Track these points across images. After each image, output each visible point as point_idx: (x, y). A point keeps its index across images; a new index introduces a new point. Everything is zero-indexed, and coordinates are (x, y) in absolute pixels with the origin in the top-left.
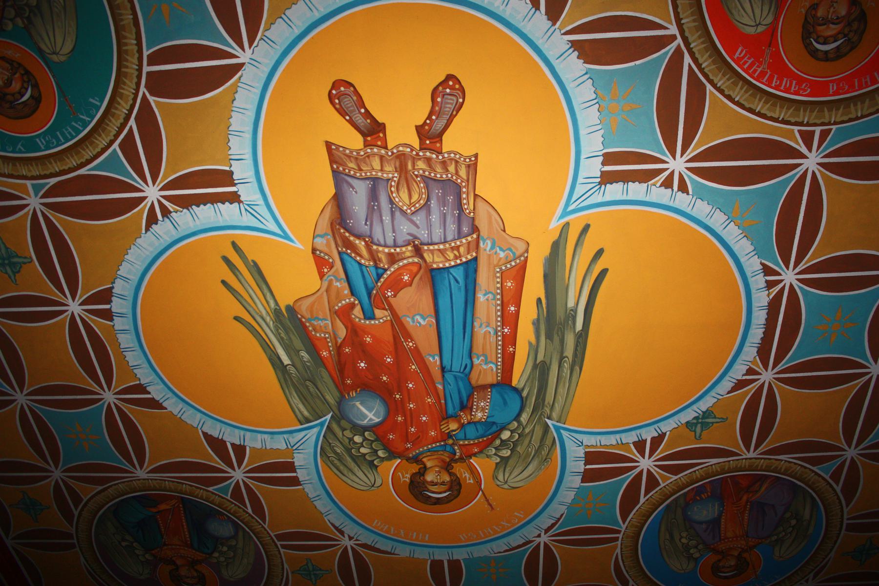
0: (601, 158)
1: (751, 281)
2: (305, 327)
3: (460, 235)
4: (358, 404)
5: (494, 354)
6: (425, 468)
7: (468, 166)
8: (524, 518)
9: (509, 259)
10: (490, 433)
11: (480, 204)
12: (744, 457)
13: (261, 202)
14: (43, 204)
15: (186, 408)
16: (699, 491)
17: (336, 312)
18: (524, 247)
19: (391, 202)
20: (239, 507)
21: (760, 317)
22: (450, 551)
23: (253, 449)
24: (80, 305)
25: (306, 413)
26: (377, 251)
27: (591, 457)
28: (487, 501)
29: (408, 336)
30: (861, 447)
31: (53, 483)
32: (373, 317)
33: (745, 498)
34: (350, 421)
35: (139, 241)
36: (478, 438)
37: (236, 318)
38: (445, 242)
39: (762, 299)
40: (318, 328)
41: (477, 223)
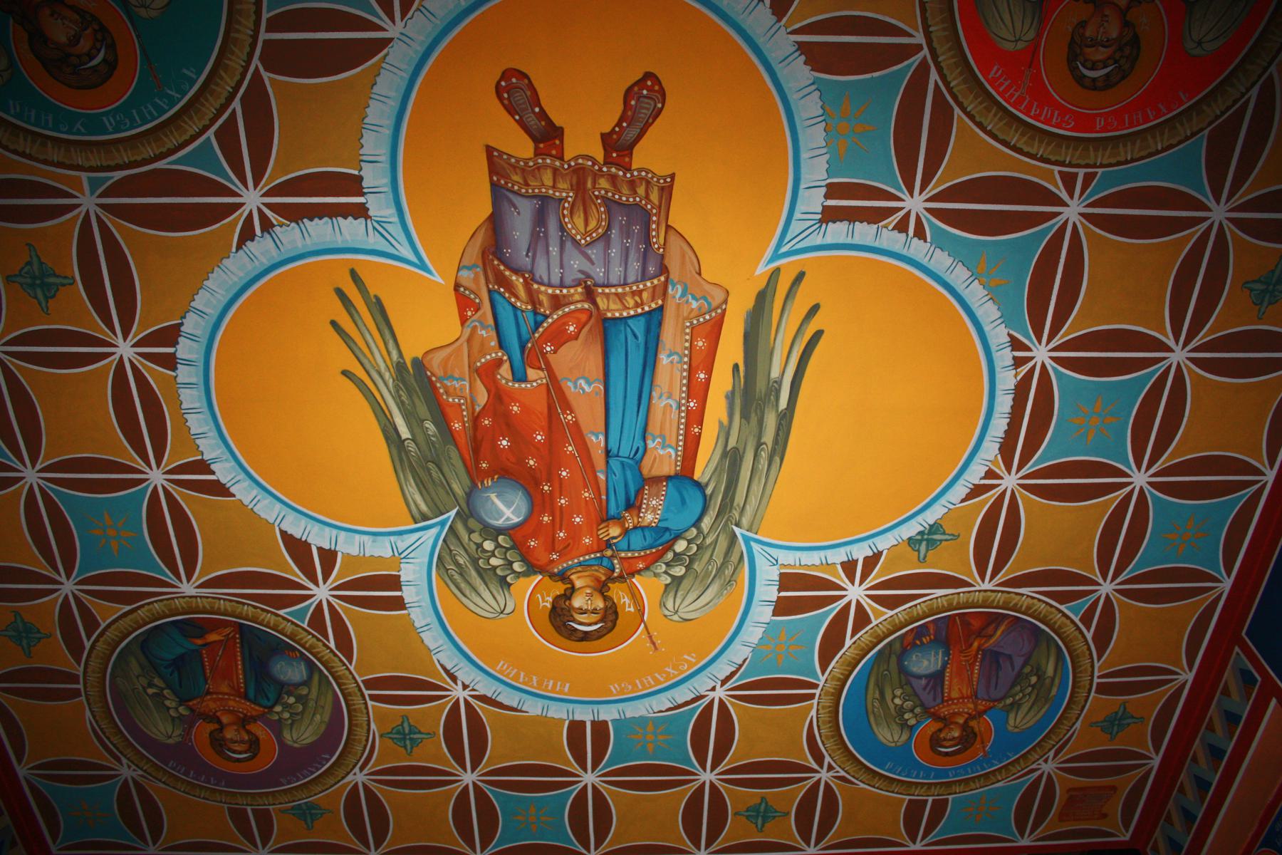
0: (824, 190)
1: (996, 355)
2: (435, 389)
3: (644, 277)
4: (493, 496)
5: (674, 435)
6: (573, 589)
7: (662, 189)
8: (695, 664)
9: (704, 311)
10: (663, 540)
11: (674, 240)
12: (977, 588)
13: (395, 219)
14: (101, 206)
15: (262, 494)
16: (920, 632)
17: (477, 371)
18: (721, 296)
19: (562, 228)
20: (319, 640)
21: (1005, 403)
22: (595, 707)
23: (347, 556)
24: (133, 346)
25: (424, 507)
26: (539, 292)
27: (787, 581)
28: (650, 637)
29: (567, 406)
30: (1118, 580)
31: (60, 601)
32: (524, 379)
33: (976, 645)
34: (481, 521)
35: (225, 262)
36: (644, 549)
37: (345, 373)
38: (625, 284)
39: (1007, 380)
40: (451, 390)
41: (666, 262)
